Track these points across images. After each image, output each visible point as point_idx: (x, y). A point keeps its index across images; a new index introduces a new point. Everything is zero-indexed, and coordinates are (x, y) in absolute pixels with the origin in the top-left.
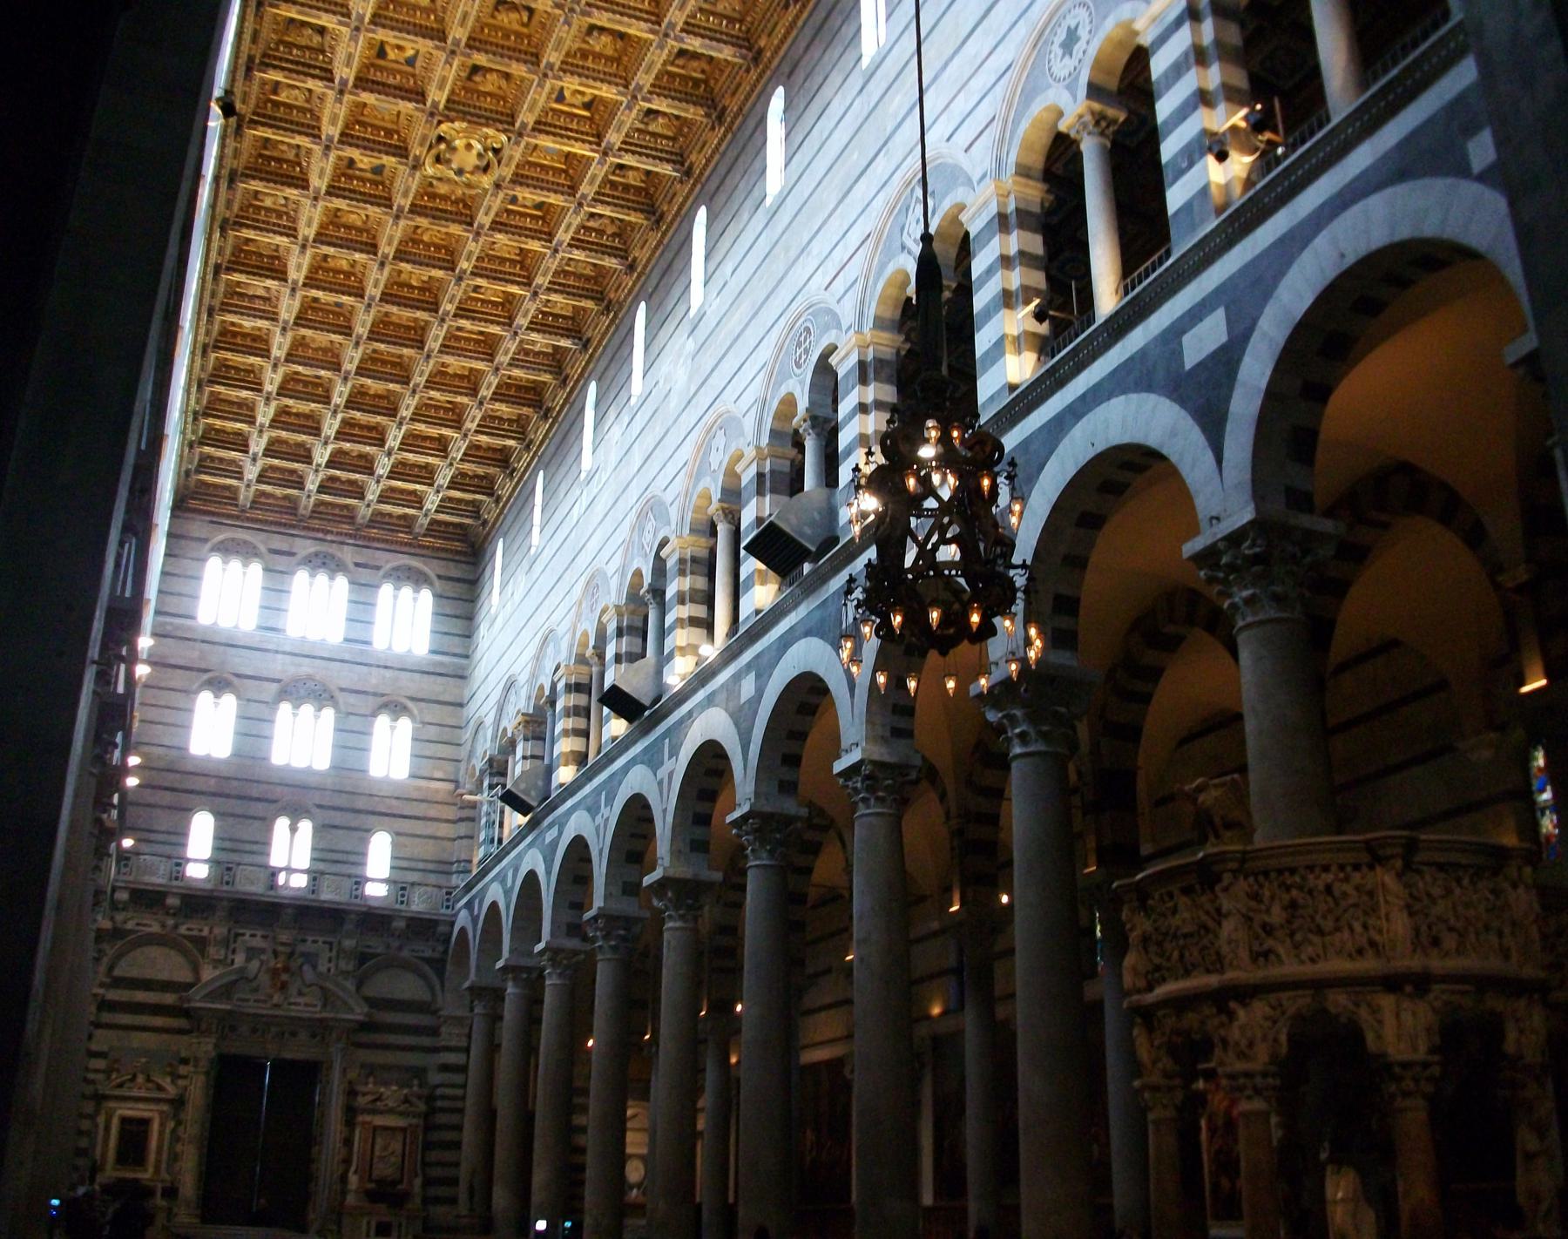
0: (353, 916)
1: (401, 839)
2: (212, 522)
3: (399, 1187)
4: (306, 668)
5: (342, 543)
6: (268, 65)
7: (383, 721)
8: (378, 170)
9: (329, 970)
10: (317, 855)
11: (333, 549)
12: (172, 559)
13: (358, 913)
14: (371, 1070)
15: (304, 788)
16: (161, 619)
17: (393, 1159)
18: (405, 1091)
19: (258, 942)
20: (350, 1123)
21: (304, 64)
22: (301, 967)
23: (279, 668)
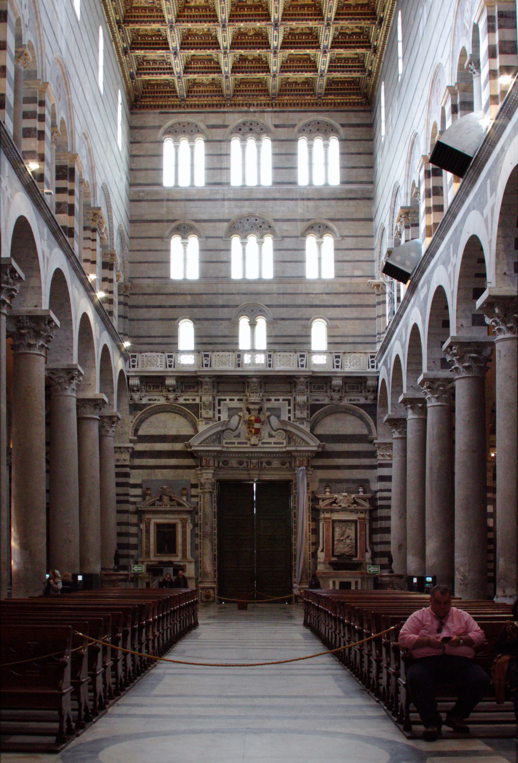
0: (302, 379)
1: (335, 323)
2: (161, 113)
3: (354, 559)
4: (247, 208)
5: (263, 112)
7: (311, 241)
9: (289, 418)
10: (272, 340)
11: (256, 118)
12: (137, 145)
13: (306, 377)
14: (328, 483)
15: (257, 294)
17: (348, 541)
18: (353, 496)
19: (236, 404)
20: (315, 519)
22: (268, 417)
23: (227, 211)
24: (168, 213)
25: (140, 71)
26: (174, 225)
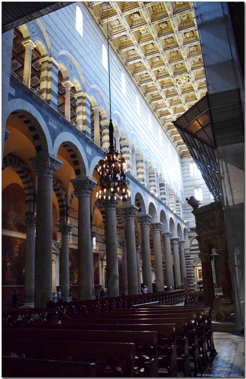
6: (141, 83)
8: (173, 90)
16: (184, 178)
21: (147, 80)
24: (193, 184)
25: (181, 149)
26: (195, 186)
